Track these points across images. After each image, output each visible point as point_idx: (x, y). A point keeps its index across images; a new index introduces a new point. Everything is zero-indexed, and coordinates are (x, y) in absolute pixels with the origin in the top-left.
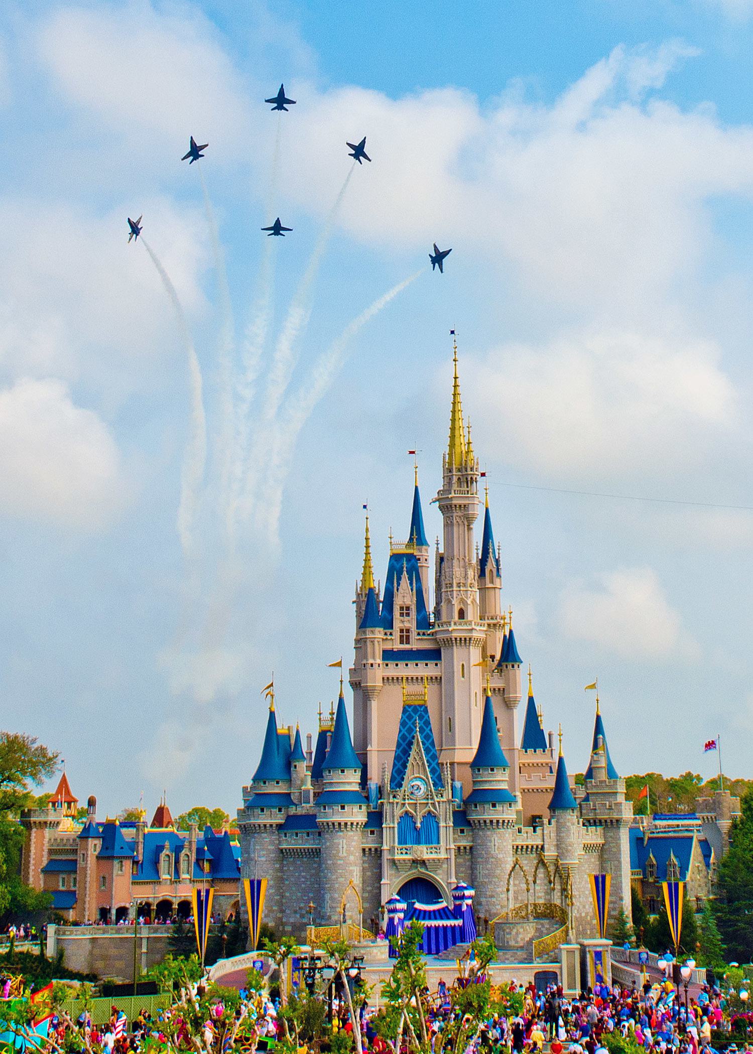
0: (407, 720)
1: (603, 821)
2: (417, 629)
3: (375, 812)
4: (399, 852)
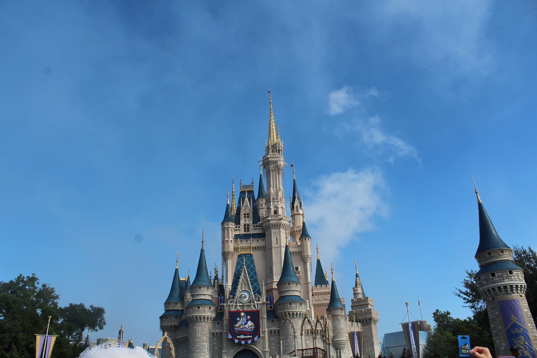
0: (240, 262)
1: (361, 320)
2: (253, 224)
3: (221, 312)
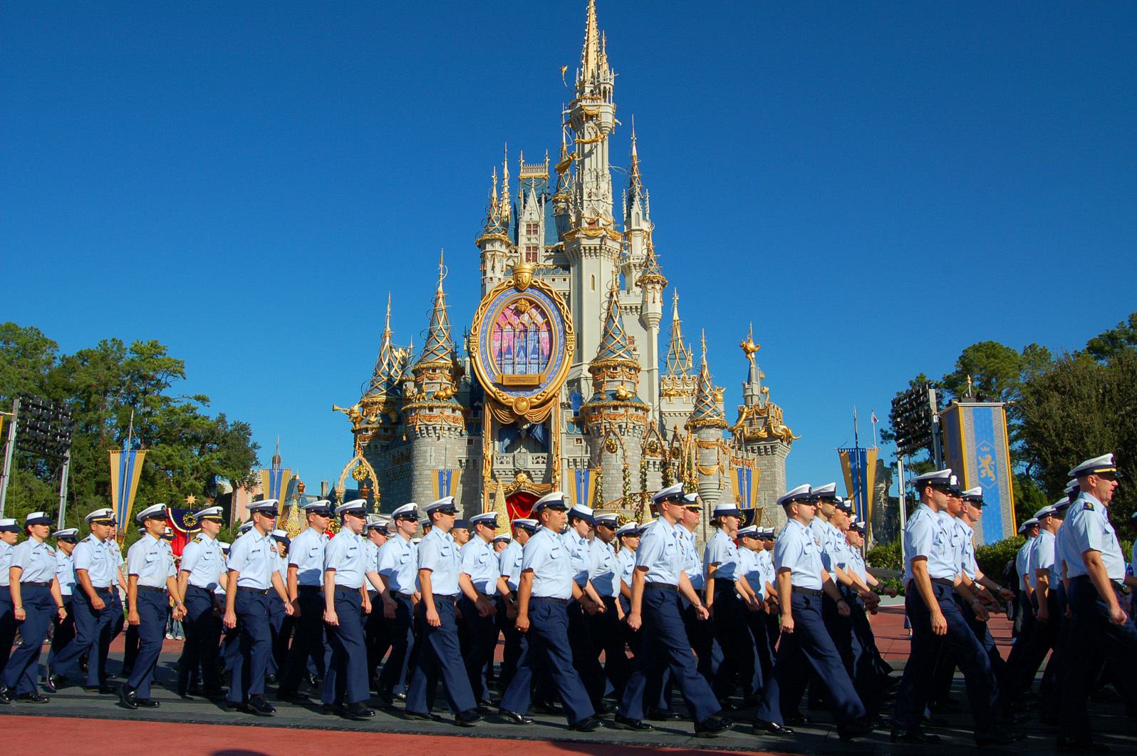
4: (499, 461)
